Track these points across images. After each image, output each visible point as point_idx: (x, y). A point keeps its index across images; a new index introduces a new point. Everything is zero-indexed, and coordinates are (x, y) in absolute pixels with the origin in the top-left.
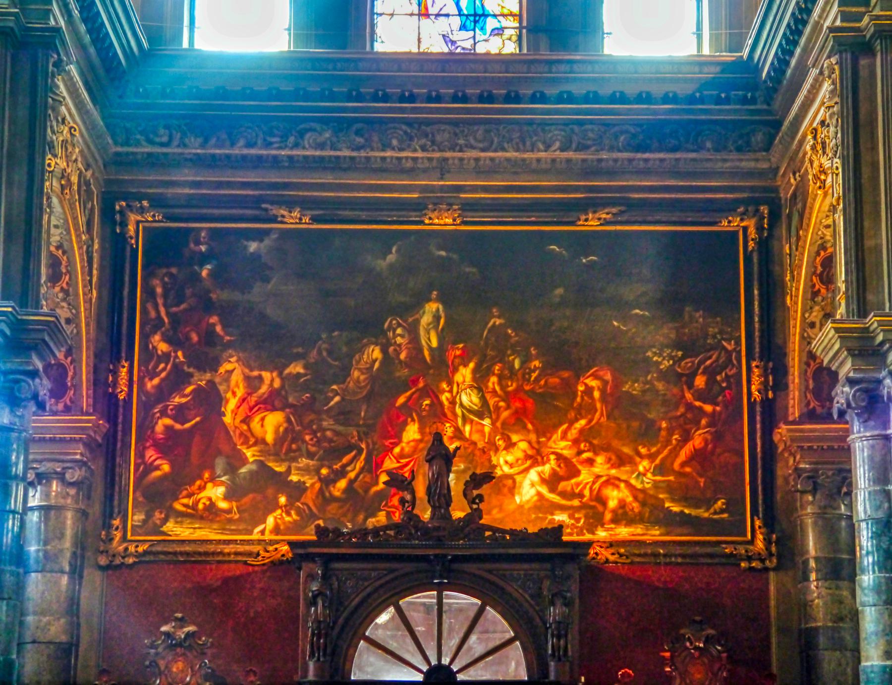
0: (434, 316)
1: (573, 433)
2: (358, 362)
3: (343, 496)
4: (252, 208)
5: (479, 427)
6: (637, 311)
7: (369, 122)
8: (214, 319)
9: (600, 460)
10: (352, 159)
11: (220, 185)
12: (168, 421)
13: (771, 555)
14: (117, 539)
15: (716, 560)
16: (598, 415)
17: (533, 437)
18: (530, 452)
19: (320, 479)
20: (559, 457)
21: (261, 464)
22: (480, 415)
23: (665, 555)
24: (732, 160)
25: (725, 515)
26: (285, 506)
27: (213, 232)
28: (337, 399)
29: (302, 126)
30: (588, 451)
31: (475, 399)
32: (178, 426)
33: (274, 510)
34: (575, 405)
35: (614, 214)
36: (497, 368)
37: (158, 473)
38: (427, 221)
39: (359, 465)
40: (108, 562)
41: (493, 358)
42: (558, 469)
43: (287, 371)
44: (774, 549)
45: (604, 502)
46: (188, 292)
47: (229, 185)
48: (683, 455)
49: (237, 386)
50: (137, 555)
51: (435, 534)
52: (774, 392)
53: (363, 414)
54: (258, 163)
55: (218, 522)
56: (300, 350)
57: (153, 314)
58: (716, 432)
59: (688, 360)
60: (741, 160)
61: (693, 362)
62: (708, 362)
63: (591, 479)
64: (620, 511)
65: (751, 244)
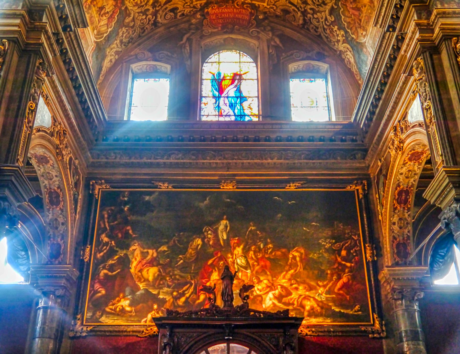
0: (225, 226)
1: (288, 276)
2: (191, 246)
3: (184, 305)
4: (148, 183)
5: (246, 274)
6: (314, 223)
7: (198, 150)
9: (301, 288)
10: (190, 163)
11: (134, 174)
12: (105, 271)
13: (383, 331)
14: (79, 324)
15: (358, 334)
16: (299, 268)
17: (270, 278)
18: (269, 285)
19: (173, 297)
20: (282, 287)
21: (146, 290)
22: (246, 268)
23: (333, 332)
24: (350, 163)
25: (360, 313)
26: (157, 309)
27: (131, 193)
28: (182, 261)
29: (170, 152)
30: (295, 284)
31: (244, 261)
32: (110, 274)
33: (151, 312)
34: (288, 263)
35: (302, 184)
36: (253, 248)
37: (100, 294)
38: (222, 188)
39: (191, 290)
40: (73, 335)
41: (251, 243)
42: (282, 292)
43: (160, 249)
44: (384, 328)
45: (303, 307)
46: (118, 216)
47: (139, 174)
49: (137, 256)
50: (88, 332)
51: (225, 314)
52: (377, 257)
53: (193, 268)
54: (150, 165)
55: (125, 317)
56: (166, 240)
57: (103, 226)
58: (353, 275)
59: (338, 244)
60: (353, 163)
61: (340, 245)
62: (347, 245)
63: (297, 297)
64: (312, 311)
65: (361, 196)
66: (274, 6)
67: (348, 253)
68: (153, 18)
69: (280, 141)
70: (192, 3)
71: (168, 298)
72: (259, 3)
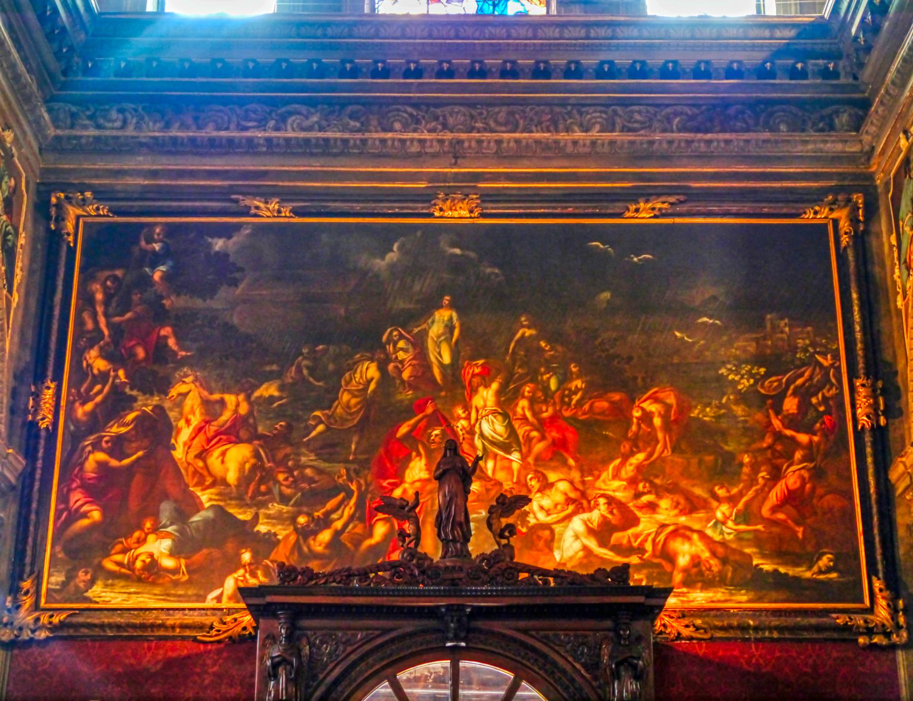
0: (446, 326)
1: (628, 470)
2: (347, 384)
3: (327, 552)
4: (218, 200)
5: (506, 463)
6: (705, 319)
7: (367, 104)
8: (166, 331)
9: (664, 504)
10: (345, 141)
11: (181, 174)
12: (101, 456)
13: (898, 627)
14: (27, 605)
15: (826, 635)
16: (659, 446)
17: (576, 475)
18: (572, 495)
19: (296, 529)
20: (611, 501)
21: (220, 511)
22: (506, 448)
23: (756, 629)
24: (815, 142)
25: (834, 575)
26: (250, 564)
27: (172, 231)
28: (321, 428)
29: (284, 109)
30: (649, 492)
31: (500, 428)
32: (114, 463)
33: (235, 570)
34: (630, 435)
35: (671, 204)
36: (527, 389)
37: (85, 522)
38: (437, 214)
39: (347, 512)
40: (12, 637)
41: (521, 377)
42: (610, 516)
43: (257, 394)
44: (901, 620)
45: (671, 558)
46: (135, 298)
47: (192, 174)
48: (774, 497)
49: (193, 412)
50: (53, 628)
51: (450, 576)
52: (886, 418)
53: (353, 447)
54: (229, 147)
55: (162, 585)
56: (275, 367)
57: (90, 325)
58: (815, 467)
59: (773, 378)
60: (825, 142)
61: (780, 381)
62: (799, 381)
63: (655, 529)
64: (694, 570)
65: (845, 240)
67: (804, 405)
69: (611, 75)
71: (282, 532)
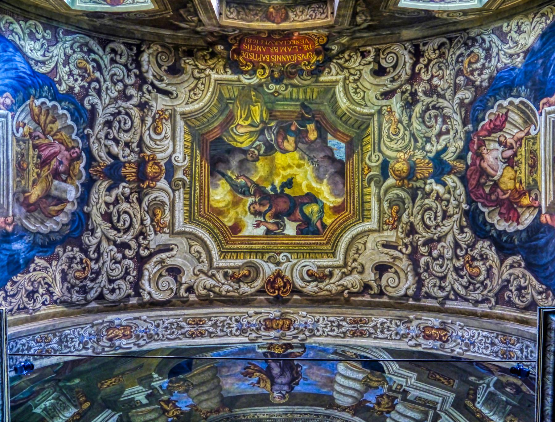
66: (198, 75)
68: (420, 70)
70: (345, 79)
72: (225, 76)
